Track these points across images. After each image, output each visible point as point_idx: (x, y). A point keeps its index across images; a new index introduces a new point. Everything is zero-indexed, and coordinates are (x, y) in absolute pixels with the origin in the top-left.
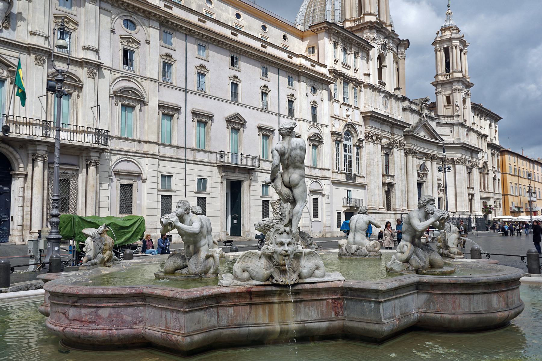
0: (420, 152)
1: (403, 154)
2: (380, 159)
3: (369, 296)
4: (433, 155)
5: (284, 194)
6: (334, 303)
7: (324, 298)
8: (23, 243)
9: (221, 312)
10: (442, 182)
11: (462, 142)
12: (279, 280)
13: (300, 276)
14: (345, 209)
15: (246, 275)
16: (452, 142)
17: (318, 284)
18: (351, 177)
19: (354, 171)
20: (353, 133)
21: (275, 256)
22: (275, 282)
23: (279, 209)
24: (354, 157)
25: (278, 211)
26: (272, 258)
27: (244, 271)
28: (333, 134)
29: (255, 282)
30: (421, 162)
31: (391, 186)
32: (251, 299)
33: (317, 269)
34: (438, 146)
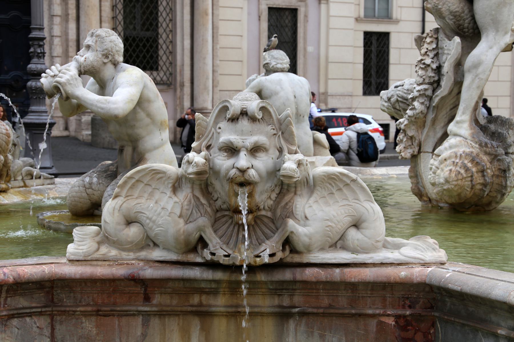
3: (494, 318)
5: (446, 14)
6: (404, 328)
7: (370, 312)
8: (65, 133)
9: (60, 330)
12: (221, 253)
13: (288, 243)
15: (133, 232)
17: (347, 270)
21: (217, 185)
22: (209, 257)
23: (431, 55)
25: (428, 61)
26: (210, 189)
27: (129, 222)
29: (157, 254)
32: (147, 299)
33: (356, 225)
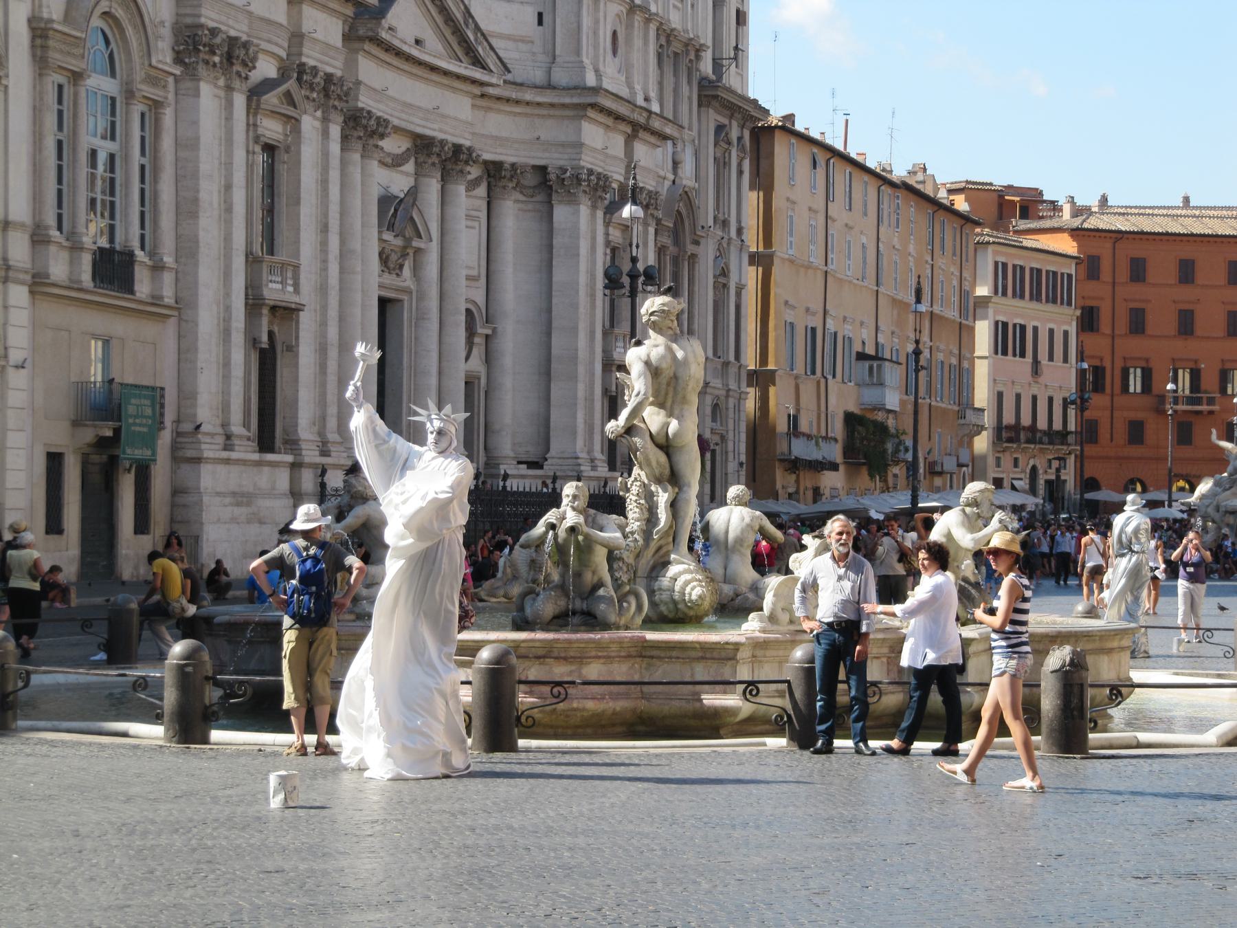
0: (398, 130)
1: (335, 147)
2: (239, 178)
4: (457, 149)
10: (480, 298)
11: (591, 81)
14: (88, 435)
16: (539, 76)
18: (113, 269)
19: (130, 234)
20: (130, 32)
24: (127, 158)
28: (40, 31)
30: (399, 182)
31: (286, 313)
34: (483, 96)
